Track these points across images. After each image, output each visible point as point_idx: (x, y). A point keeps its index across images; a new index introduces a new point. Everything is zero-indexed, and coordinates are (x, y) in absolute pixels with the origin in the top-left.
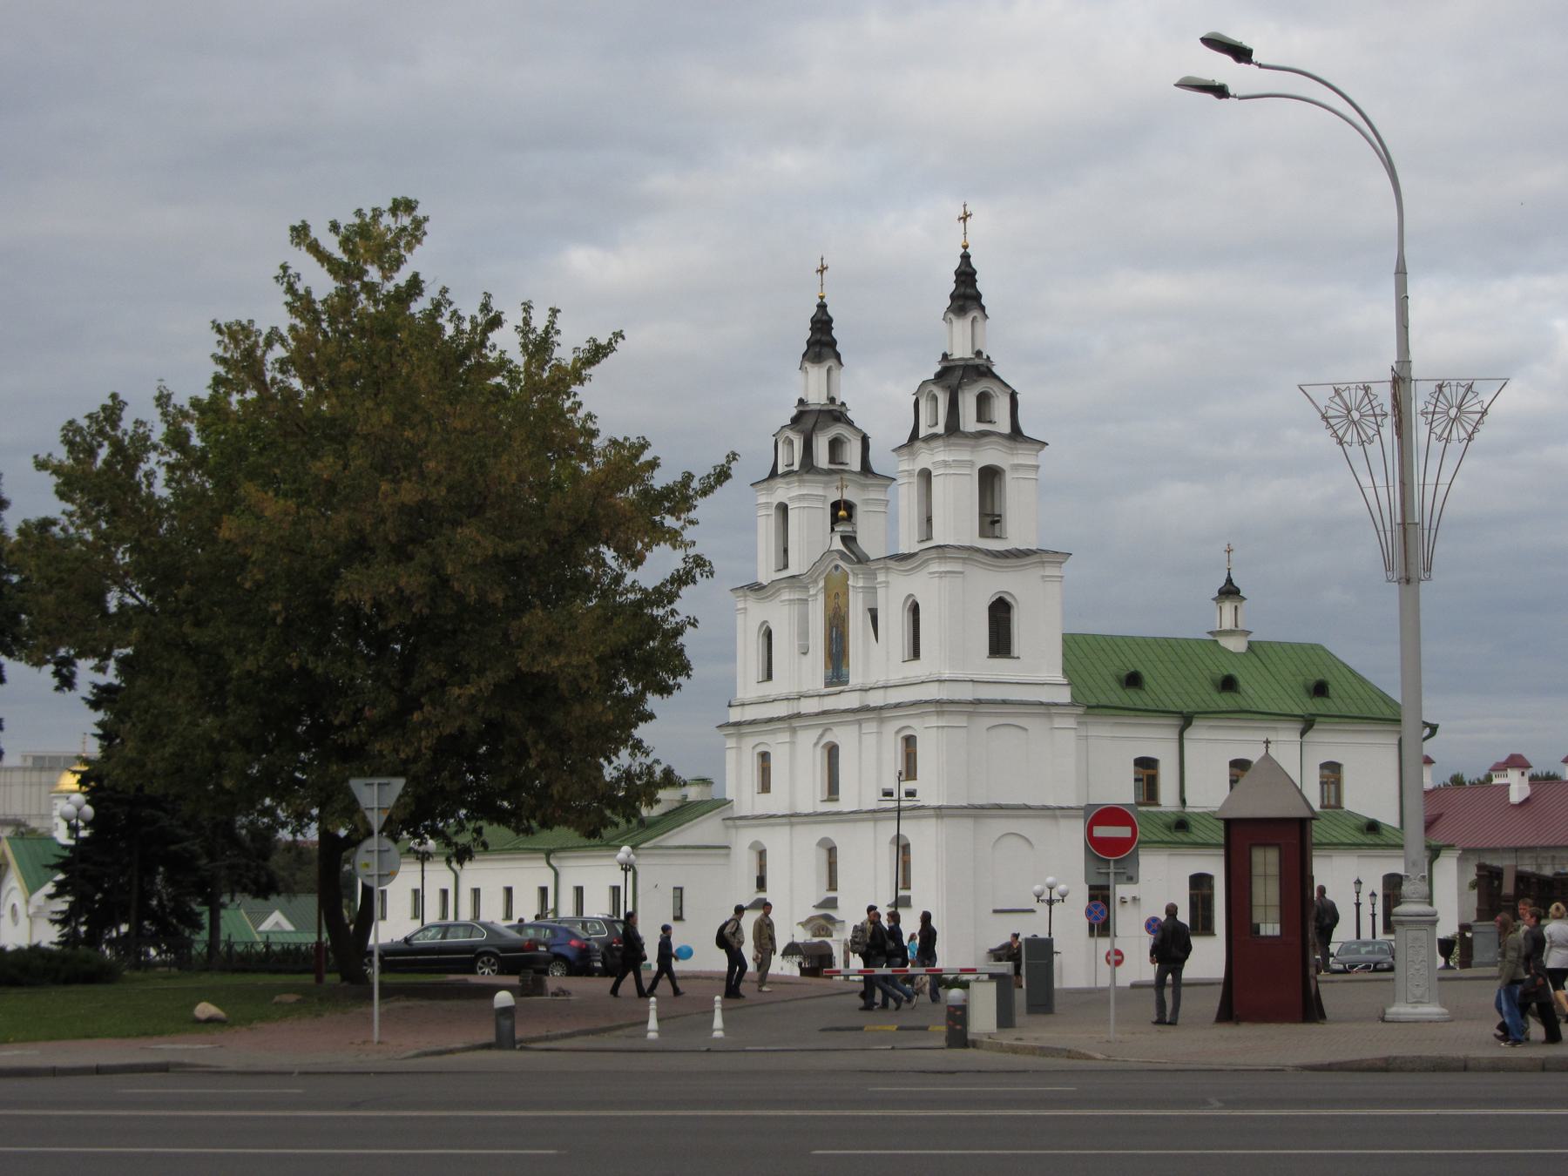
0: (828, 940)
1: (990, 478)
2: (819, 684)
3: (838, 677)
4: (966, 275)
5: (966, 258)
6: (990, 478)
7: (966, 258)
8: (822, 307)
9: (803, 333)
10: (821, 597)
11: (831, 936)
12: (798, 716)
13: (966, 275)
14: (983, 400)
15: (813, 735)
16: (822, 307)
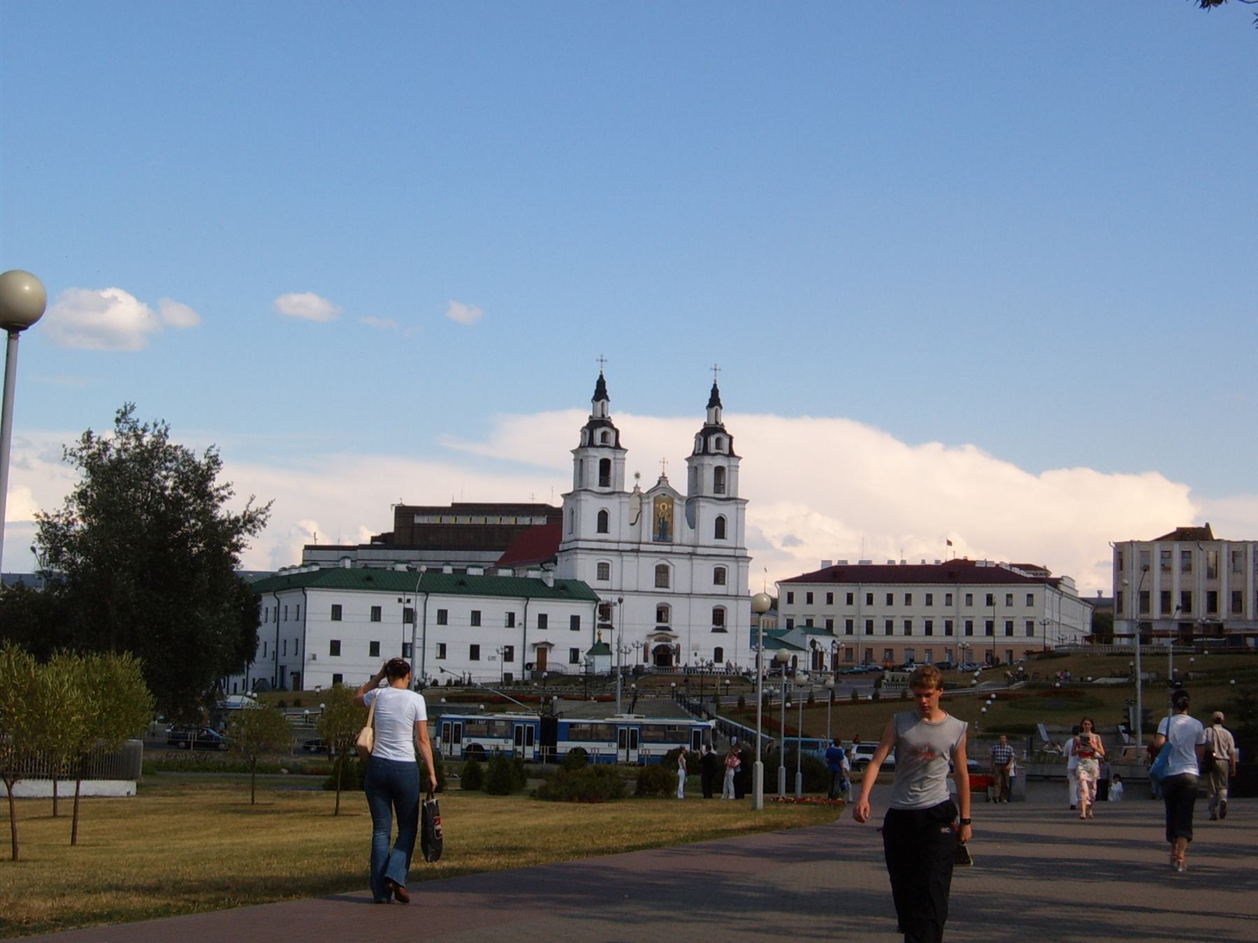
0: (669, 643)
1: (719, 471)
2: (651, 541)
3: (664, 538)
4: (715, 392)
5: (715, 385)
6: (719, 471)
7: (715, 385)
8: (601, 377)
9: (593, 387)
10: (652, 504)
11: (670, 641)
12: (638, 551)
13: (715, 392)
14: (718, 441)
15: (654, 560)
16: (601, 377)
